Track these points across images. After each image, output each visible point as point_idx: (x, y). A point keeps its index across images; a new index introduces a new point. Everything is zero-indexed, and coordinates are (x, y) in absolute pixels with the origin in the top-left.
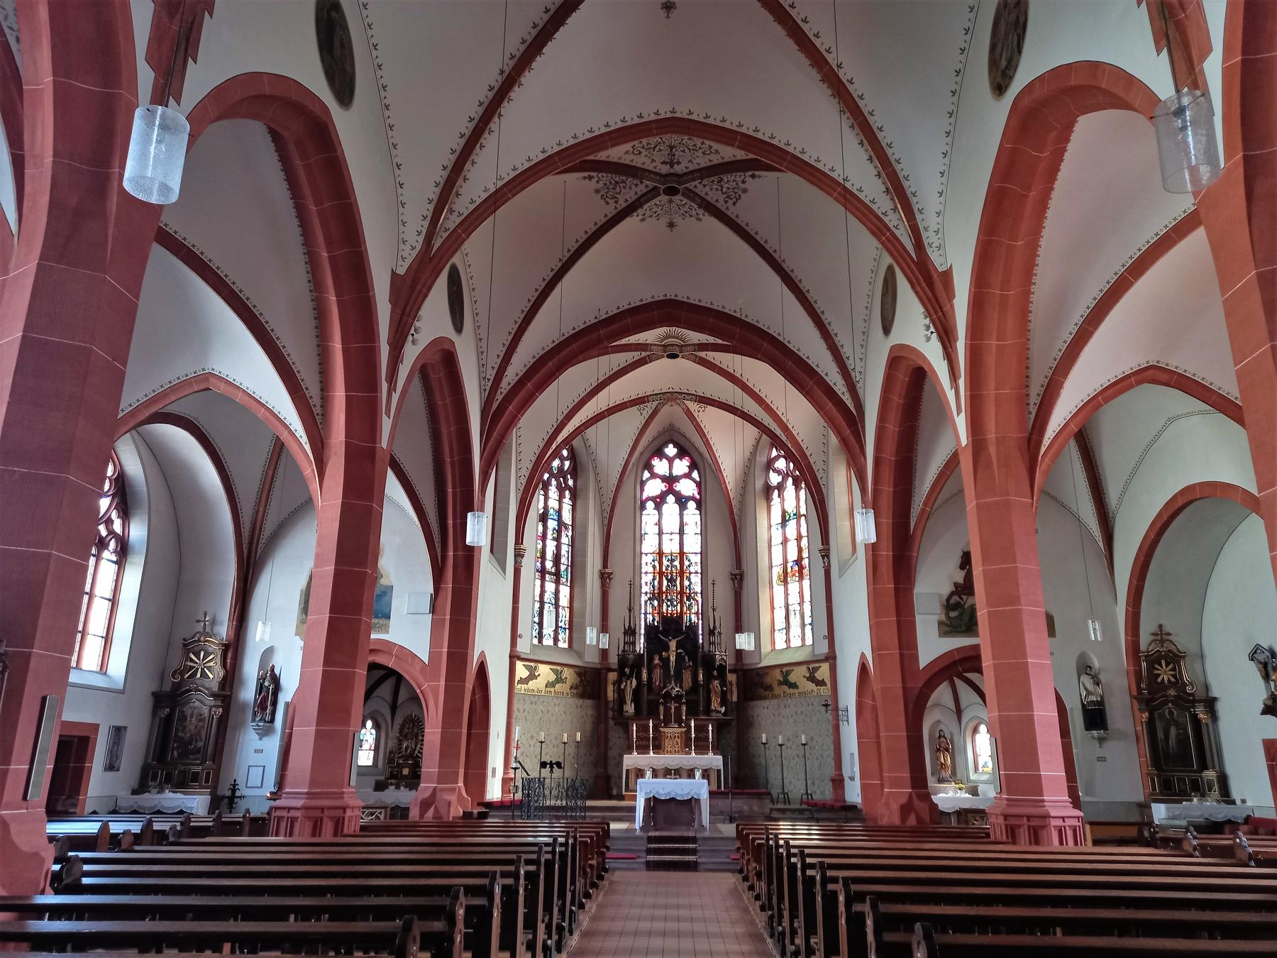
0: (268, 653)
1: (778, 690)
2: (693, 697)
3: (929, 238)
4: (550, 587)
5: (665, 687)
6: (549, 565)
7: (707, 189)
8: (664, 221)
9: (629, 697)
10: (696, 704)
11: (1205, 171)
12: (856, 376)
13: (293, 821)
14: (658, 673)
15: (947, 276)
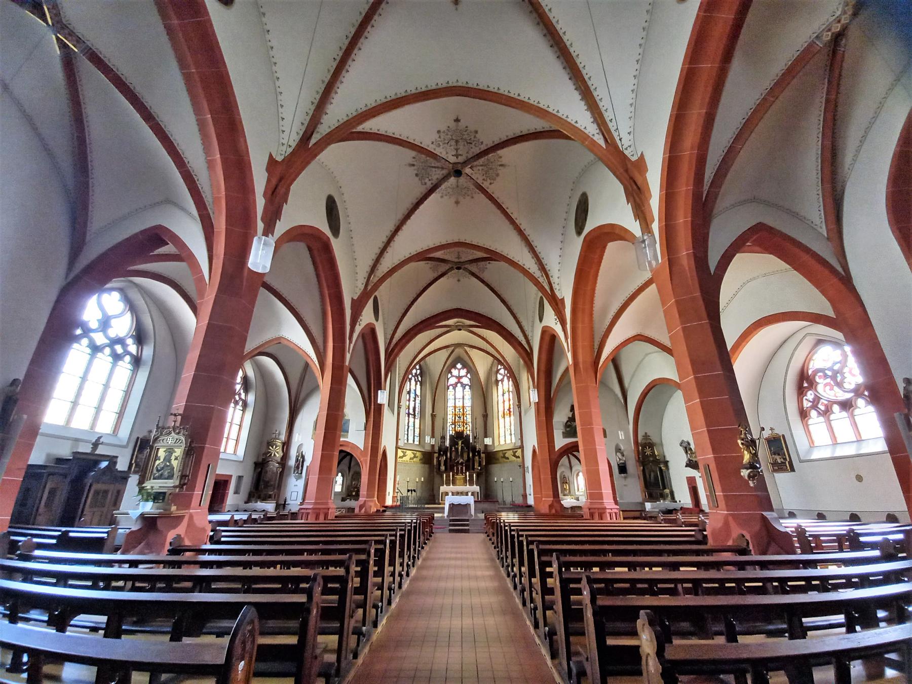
0: (300, 446)
1: (501, 460)
3: (555, 286)
4: (411, 419)
6: (411, 411)
8: (456, 279)
10: (469, 466)
11: (654, 263)
12: (530, 338)
13: (308, 514)
15: (563, 300)
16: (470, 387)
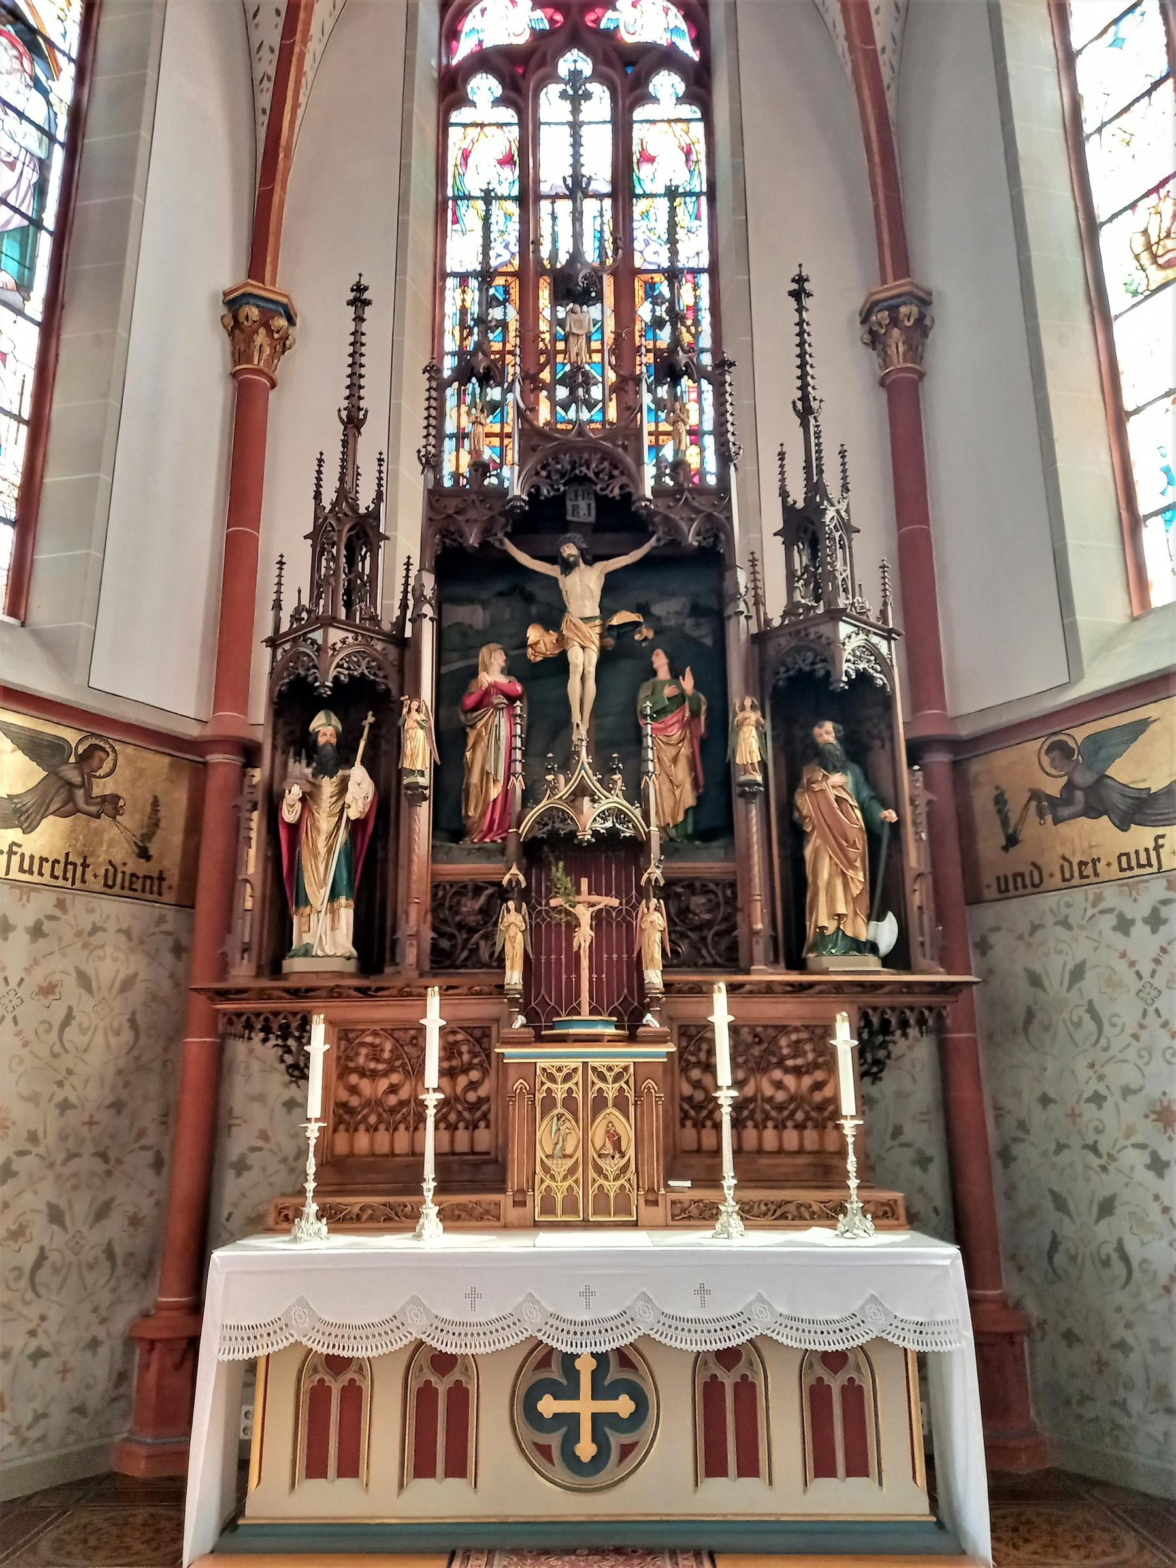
2: (706, 864)
5: (530, 796)
9: (320, 868)
14: (497, 740)
16: (699, 86)
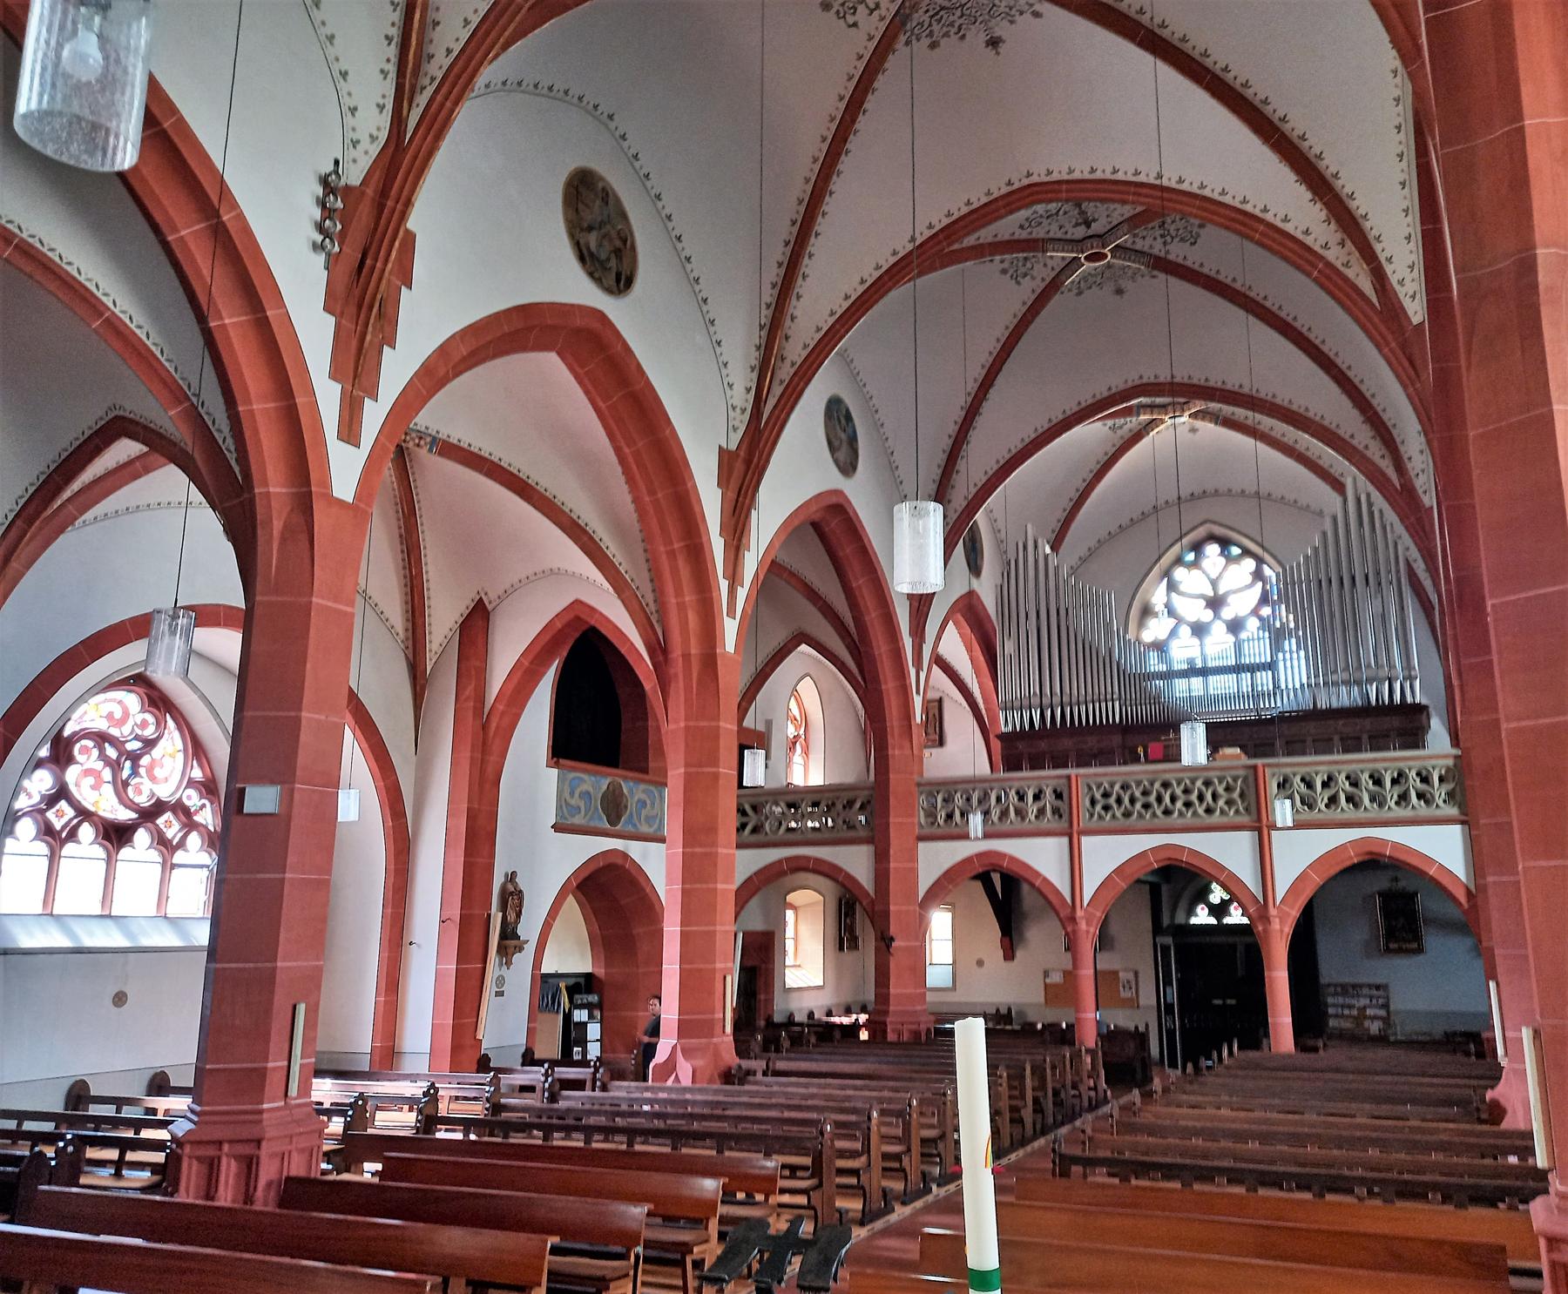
7: (1149, 241)
